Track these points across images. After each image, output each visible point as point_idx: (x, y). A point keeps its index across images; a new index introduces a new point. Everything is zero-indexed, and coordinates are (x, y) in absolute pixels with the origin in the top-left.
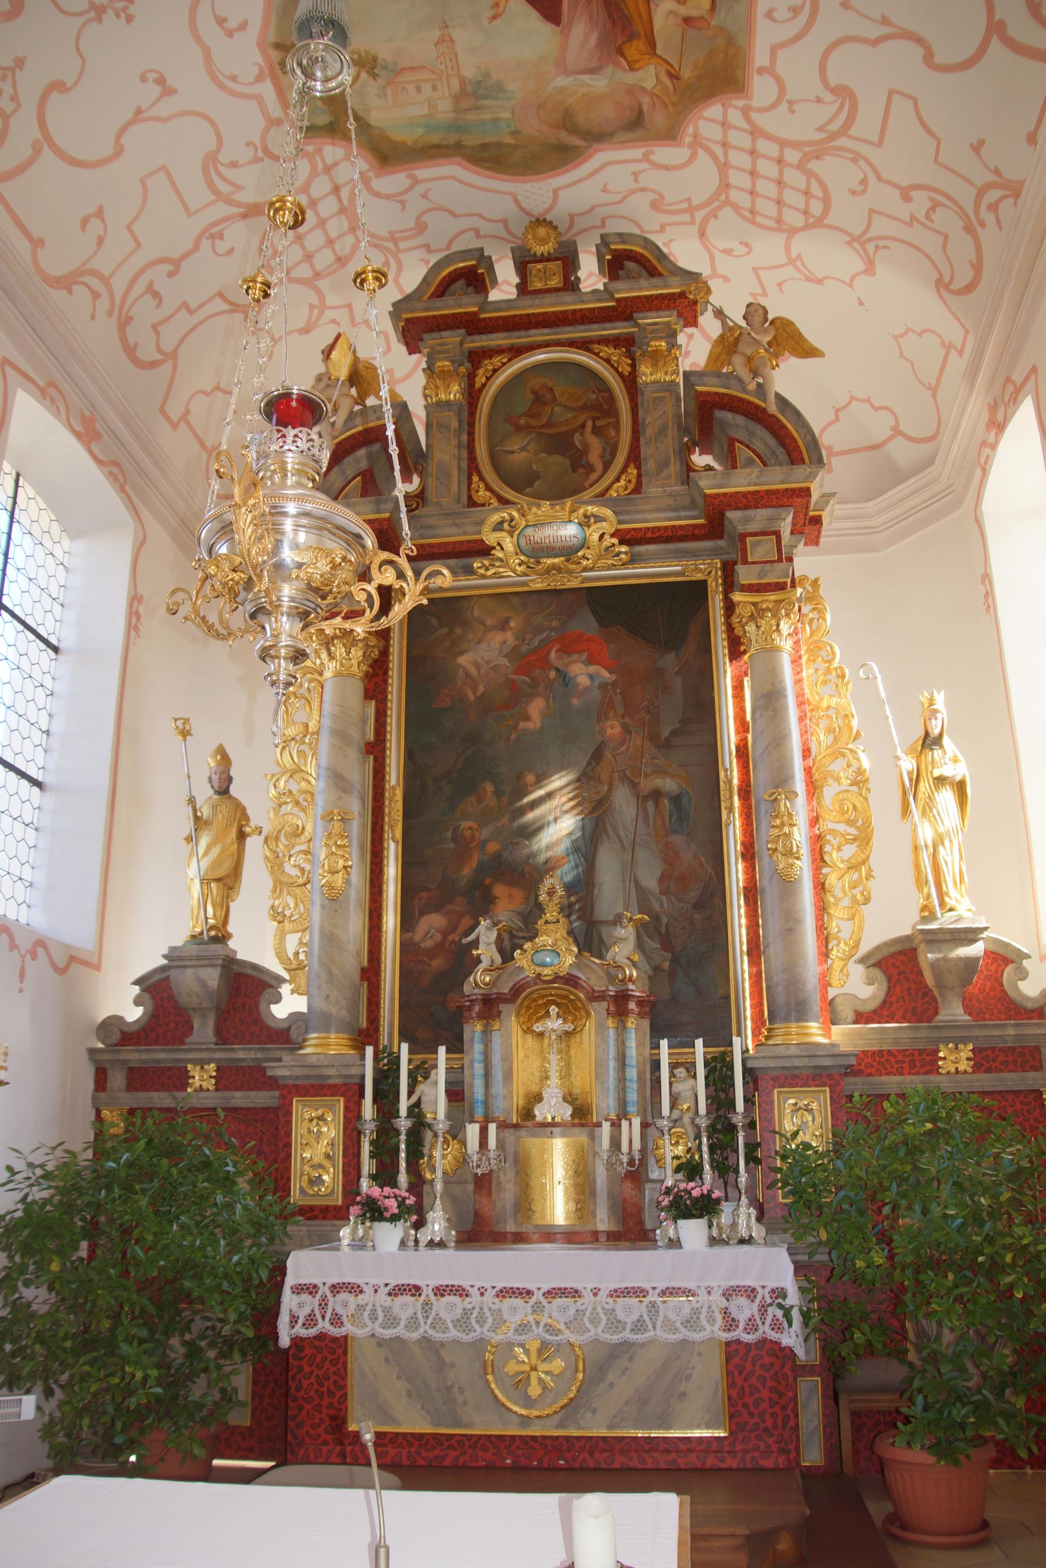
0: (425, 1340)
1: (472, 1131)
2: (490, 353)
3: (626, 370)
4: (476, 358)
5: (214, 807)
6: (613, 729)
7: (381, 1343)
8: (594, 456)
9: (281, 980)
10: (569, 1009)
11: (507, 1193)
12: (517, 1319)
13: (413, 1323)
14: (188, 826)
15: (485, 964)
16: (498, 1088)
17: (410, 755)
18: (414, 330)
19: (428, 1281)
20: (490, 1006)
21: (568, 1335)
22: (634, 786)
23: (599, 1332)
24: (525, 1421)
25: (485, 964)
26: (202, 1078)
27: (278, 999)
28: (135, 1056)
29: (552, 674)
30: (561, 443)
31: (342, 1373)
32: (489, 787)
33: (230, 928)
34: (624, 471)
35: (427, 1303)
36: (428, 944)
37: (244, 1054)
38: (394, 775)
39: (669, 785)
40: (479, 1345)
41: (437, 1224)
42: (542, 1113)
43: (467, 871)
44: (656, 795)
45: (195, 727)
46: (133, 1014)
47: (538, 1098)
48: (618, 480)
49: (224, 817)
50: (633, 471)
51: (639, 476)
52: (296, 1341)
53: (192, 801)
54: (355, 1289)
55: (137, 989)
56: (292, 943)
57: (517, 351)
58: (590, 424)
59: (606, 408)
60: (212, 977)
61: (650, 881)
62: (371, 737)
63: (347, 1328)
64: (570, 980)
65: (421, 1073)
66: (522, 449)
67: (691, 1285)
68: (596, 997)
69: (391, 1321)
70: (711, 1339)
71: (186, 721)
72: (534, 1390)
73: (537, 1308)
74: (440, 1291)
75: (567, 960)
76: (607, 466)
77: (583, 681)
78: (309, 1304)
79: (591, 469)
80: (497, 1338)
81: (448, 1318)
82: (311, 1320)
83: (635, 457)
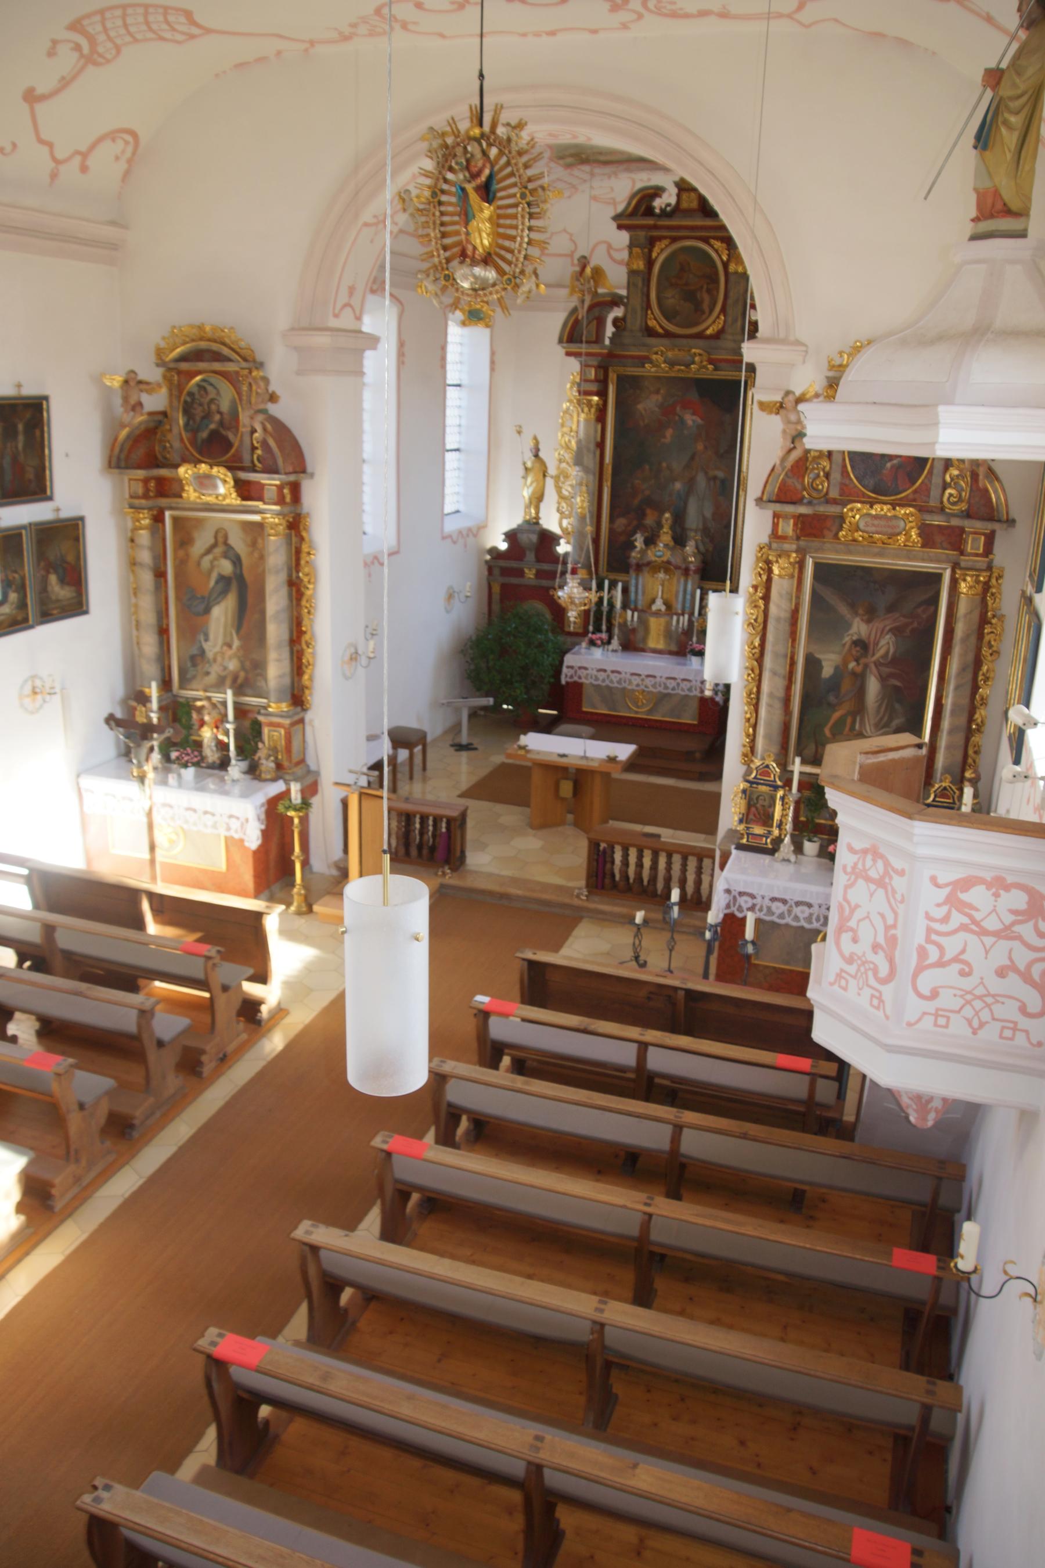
0: (607, 687)
1: (629, 613)
2: (660, 239)
3: (725, 258)
4: (652, 242)
5: (533, 463)
6: (700, 446)
7: (594, 685)
8: (705, 306)
9: (560, 537)
10: (667, 571)
11: (640, 635)
12: (635, 683)
13: (604, 681)
14: (522, 472)
15: (638, 549)
16: (640, 597)
17: (616, 448)
18: (622, 221)
19: (609, 668)
20: (639, 568)
21: (651, 689)
22: (706, 473)
23: (661, 689)
24: (637, 713)
25: (638, 549)
26: (530, 574)
27: (559, 544)
28: (503, 563)
29: (677, 418)
30: (690, 296)
31: (580, 694)
32: (647, 467)
33: (541, 515)
34: (718, 317)
35: (608, 676)
36: (619, 530)
37: (546, 567)
38: (608, 458)
39: (720, 474)
40: (624, 689)
41: (615, 643)
42: (654, 608)
43: (636, 502)
44: (715, 478)
45: (524, 430)
46: (503, 546)
47: (653, 601)
48: (714, 322)
49: (538, 466)
50: (722, 318)
51: (725, 322)
52: (567, 683)
53: (524, 464)
54: (586, 668)
55: (503, 537)
56: (565, 523)
57: (674, 240)
58: (705, 287)
59: (714, 279)
60: (534, 538)
61: (708, 514)
62: (599, 439)
63: (583, 680)
64: (668, 562)
65: (613, 585)
66: (673, 297)
67: (690, 678)
68: (677, 568)
69: (597, 679)
70: (695, 696)
71: (520, 427)
72: (640, 704)
73: (643, 680)
74: (613, 672)
75: (668, 555)
76: (711, 311)
77: (690, 423)
78: (571, 672)
79: (703, 313)
80: (630, 687)
81: (615, 680)
82: (571, 677)
83: (723, 310)
